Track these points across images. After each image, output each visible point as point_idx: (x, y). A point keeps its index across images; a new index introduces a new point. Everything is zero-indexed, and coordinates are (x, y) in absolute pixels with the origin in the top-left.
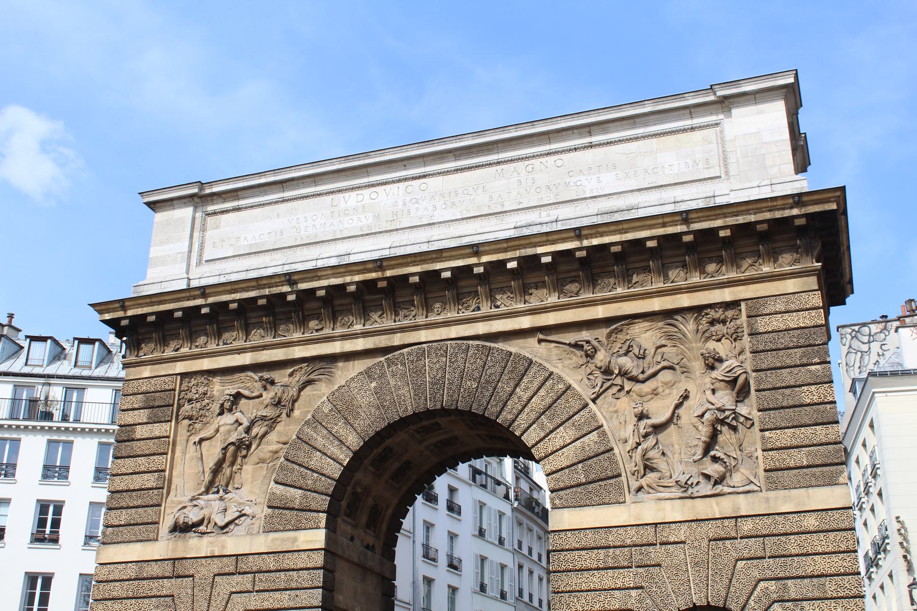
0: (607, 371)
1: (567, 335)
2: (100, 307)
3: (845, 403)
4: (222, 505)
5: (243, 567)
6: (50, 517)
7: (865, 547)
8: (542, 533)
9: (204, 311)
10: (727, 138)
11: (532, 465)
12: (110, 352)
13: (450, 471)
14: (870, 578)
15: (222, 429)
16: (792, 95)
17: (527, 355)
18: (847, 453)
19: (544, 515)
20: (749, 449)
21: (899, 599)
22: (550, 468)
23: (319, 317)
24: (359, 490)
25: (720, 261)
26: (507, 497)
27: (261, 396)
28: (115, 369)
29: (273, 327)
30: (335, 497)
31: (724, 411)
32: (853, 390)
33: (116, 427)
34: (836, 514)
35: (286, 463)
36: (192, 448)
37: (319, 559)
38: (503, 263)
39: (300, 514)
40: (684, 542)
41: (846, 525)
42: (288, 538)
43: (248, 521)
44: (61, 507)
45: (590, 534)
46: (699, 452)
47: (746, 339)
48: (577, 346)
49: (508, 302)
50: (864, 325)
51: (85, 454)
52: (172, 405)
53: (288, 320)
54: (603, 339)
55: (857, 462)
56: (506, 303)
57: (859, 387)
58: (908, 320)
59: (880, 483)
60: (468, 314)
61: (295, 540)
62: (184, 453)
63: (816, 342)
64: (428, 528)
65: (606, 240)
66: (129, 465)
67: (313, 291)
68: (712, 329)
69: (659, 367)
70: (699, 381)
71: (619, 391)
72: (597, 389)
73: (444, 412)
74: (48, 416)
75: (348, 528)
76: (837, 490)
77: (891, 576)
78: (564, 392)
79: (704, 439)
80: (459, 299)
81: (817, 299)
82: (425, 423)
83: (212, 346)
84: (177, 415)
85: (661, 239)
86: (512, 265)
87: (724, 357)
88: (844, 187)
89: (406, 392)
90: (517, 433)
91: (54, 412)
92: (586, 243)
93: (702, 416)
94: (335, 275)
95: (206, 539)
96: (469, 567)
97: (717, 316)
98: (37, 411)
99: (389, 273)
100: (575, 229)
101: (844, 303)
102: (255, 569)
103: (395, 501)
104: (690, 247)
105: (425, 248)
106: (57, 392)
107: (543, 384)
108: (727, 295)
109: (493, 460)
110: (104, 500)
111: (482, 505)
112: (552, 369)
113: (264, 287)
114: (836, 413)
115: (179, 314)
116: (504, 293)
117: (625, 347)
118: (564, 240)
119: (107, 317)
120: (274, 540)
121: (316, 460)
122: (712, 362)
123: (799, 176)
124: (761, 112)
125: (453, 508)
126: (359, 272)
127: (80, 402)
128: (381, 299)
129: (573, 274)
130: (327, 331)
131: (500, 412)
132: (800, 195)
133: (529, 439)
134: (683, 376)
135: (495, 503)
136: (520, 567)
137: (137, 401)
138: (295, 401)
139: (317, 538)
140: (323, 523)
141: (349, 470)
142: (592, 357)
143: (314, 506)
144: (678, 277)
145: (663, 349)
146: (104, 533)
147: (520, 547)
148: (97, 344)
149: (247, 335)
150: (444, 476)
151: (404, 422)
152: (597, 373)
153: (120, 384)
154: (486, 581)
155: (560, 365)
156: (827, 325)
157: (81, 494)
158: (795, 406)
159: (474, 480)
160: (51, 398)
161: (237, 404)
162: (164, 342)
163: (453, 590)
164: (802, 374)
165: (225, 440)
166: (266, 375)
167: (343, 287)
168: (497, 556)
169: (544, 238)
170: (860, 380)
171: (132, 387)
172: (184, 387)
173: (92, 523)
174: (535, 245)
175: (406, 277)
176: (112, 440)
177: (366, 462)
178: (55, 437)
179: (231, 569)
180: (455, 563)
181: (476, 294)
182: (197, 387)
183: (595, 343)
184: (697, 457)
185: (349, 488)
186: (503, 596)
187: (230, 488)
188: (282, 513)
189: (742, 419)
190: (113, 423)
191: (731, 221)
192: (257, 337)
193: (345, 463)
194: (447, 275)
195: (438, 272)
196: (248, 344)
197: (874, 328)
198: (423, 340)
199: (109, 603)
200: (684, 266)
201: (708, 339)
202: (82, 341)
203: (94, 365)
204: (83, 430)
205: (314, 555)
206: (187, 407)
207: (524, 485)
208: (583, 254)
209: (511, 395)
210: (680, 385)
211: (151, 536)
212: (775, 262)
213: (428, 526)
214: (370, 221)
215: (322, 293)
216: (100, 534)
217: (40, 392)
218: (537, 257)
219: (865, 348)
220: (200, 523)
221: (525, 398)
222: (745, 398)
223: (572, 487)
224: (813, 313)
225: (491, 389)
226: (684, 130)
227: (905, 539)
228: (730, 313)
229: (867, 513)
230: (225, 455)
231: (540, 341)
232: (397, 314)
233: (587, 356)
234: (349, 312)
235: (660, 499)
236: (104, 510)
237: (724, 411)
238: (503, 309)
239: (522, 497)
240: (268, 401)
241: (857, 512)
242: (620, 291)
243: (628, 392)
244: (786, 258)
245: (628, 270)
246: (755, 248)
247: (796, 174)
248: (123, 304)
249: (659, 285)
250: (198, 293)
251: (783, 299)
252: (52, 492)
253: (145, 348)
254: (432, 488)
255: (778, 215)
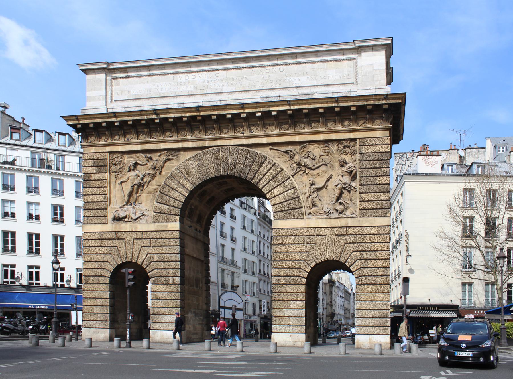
0: (299, 164)
1: (283, 147)
2: (67, 118)
3: (393, 184)
4: (134, 210)
5: (145, 236)
6: (58, 212)
7: (393, 241)
8: (269, 229)
9: (116, 124)
10: (358, 66)
11: (266, 201)
12: (74, 140)
13: (231, 202)
14: (393, 253)
15: (130, 178)
16: (389, 49)
17: (265, 155)
18: (391, 205)
19: (270, 222)
20: (354, 201)
21: (402, 261)
22: (273, 203)
23: (170, 131)
24: (193, 207)
25: (350, 121)
26: (255, 214)
27: (147, 164)
28: (77, 148)
29: (150, 134)
30: (183, 209)
31: (346, 184)
32: (397, 180)
33: (82, 174)
34: (384, 228)
35: (160, 194)
36: (118, 185)
37: (177, 234)
38: (255, 113)
39: (168, 216)
40: (326, 235)
41: (387, 232)
42: (164, 226)
43: (146, 217)
44: (63, 208)
45: (289, 230)
46: (335, 200)
47: (358, 155)
48: (286, 152)
49: (257, 131)
50: (405, 153)
51: (69, 186)
52: (107, 166)
53: (157, 131)
54: (298, 150)
55: (394, 209)
56: (256, 131)
57: (399, 179)
58: (422, 153)
59: (402, 216)
60: (239, 135)
61: (167, 226)
62: (115, 187)
63: (385, 159)
64: (222, 225)
65: (301, 107)
66: (90, 191)
67: (167, 119)
68: (344, 150)
69: (321, 164)
70: (337, 171)
71: (304, 173)
72: (294, 171)
73: (228, 176)
74: (50, 167)
75: (189, 223)
76: (386, 219)
77: (400, 252)
78: (280, 172)
79: (337, 195)
80: (234, 128)
81: (388, 141)
82: (220, 181)
83: (122, 141)
84: (110, 171)
85: (326, 108)
86: (259, 114)
87: (348, 162)
88: (406, 93)
89: (212, 167)
90: (260, 188)
91: (52, 165)
92: (292, 107)
93: (337, 186)
94: (177, 112)
95: (128, 224)
96: (239, 241)
97: (346, 144)
98: (44, 165)
99: (202, 114)
100: (288, 101)
101: (399, 143)
102: (150, 237)
103: (208, 213)
104: (338, 113)
105: (219, 103)
106: (52, 157)
107: (271, 168)
108: (351, 136)
109: (249, 198)
110: (82, 206)
111: (245, 217)
112: (275, 161)
113: (144, 115)
114: (390, 188)
115: (104, 125)
116: (255, 127)
117: (307, 155)
118: (283, 105)
119: (70, 123)
120: (158, 226)
121: (173, 194)
122: (343, 164)
123: (388, 86)
124: (374, 55)
125: (232, 217)
126: (188, 112)
127: (63, 162)
128: (199, 125)
129: (286, 121)
130: (175, 138)
131: (253, 178)
132: (387, 95)
133: (265, 190)
134: (330, 169)
135: (250, 216)
136: (260, 242)
137: (90, 163)
138: (162, 168)
139: (176, 226)
140: (178, 220)
141: (188, 199)
142: (293, 158)
143: (174, 213)
144: (331, 126)
145: (323, 157)
146: (84, 219)
147: (260, 234)
148: (67, 135)
149: (138, 136)
150: (228, 204)
151: (211, 180)
152: (295, 165)
153: (81, 155)
154: (246, 247)
155: (279, 160)
156: (391, 152)
157: (71, 203)
158: (374, 184)
159: (241, 206)
160: (49, 159)
161: (136, 167)
162: (99, 137)
163: (233, 250)
164: (378, 172)
165: (132, 183)
166: (148, 155)
167: (181, 118)
168: (251, 237)
169: (274, 104)
170: (400, 176)
171: (87, 156)
172: (111, 158)
173: (78, 215)
174: (270, 106)
175: (210, 116)
176: (81, 180)
177: (196, 196)
178: (55, 177)
179: (141, 237)
180: (234, 239)
181: (242, 126)
182: (117, 159)
183: (294, 152)
184: (333, 202)
185: (189, 206)
186: (253, 253)
187: (137, 203)
188: (160, 215)
189: (352, 188)
190: (80, 172)
191: (356, 103)
192: (143, 138)
193: (186, 196)
194: (229, 116)
195: (225, 115)
196: (139, 141)
197: (409, 155)
198: (219, 145)
199: (91, 248)
200: (334, 121)
201: (342, 154)
202: (60, 134)
203: (67, 145)
204: (67, 174)
205: (175, 233)
206: (113, 167)
207: (262, 210)
208: (291, 112)
209: (257, 171)
210: (329, 172)
211: (105, 222)
212: (373, 123)
213: (222, 224)
214: (192, 89)
215: (171, 120)
216: (82, 220)
217: (44, 156)
218: (270, 112)
219: (404, 163)
220: (125, 217)
221: (263, 173)
222: (355, 179)
223: (282, 211)
224: (386, 146)
225: (249, 168)
226: (340, 60)
227: (408, 239)
228: (352, 144)
229: (395, 228)
230: (133, 189)
231: (270, 149)
232: (206, 132)
233: (291, 157)
234: (185, 130)
235: (317, 218)
236: (82, 210)
237: (346, 184)
238: (254, 134)
239: (261, 214)
240: (150, 167)
241: (391, 228)
242: (306, 130)
243: (307, 174)
244: (378, 122)
245: (310, 121)
246: (365, 116)
247: (387, 84)
248: (77, 118)
249: (324, 129)
250: (112, 115)
251: (375, 139)
252: (58, 201)
253: (91, 139)
254: (224, 208)
255: (377, 102)
